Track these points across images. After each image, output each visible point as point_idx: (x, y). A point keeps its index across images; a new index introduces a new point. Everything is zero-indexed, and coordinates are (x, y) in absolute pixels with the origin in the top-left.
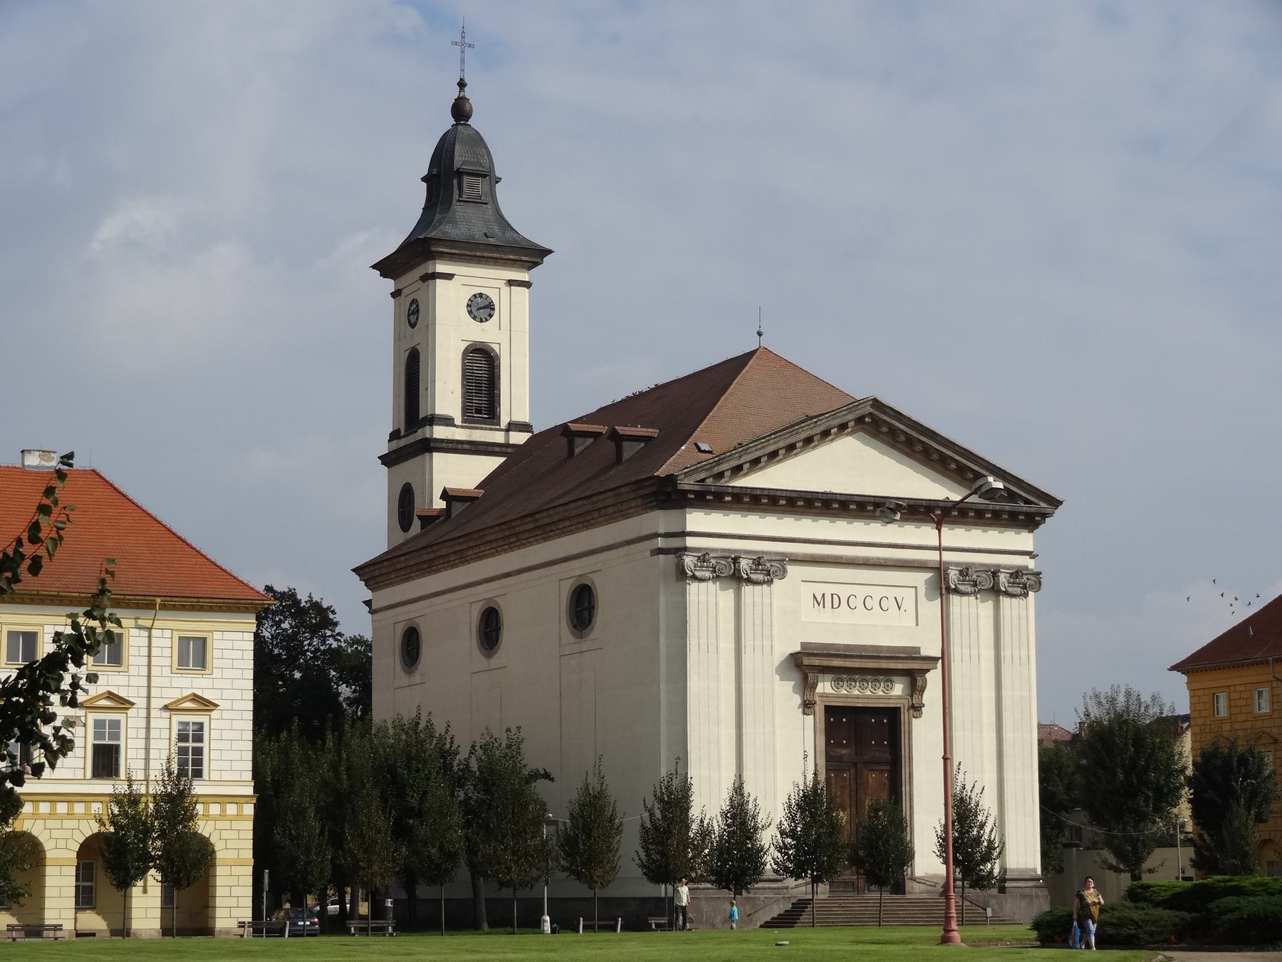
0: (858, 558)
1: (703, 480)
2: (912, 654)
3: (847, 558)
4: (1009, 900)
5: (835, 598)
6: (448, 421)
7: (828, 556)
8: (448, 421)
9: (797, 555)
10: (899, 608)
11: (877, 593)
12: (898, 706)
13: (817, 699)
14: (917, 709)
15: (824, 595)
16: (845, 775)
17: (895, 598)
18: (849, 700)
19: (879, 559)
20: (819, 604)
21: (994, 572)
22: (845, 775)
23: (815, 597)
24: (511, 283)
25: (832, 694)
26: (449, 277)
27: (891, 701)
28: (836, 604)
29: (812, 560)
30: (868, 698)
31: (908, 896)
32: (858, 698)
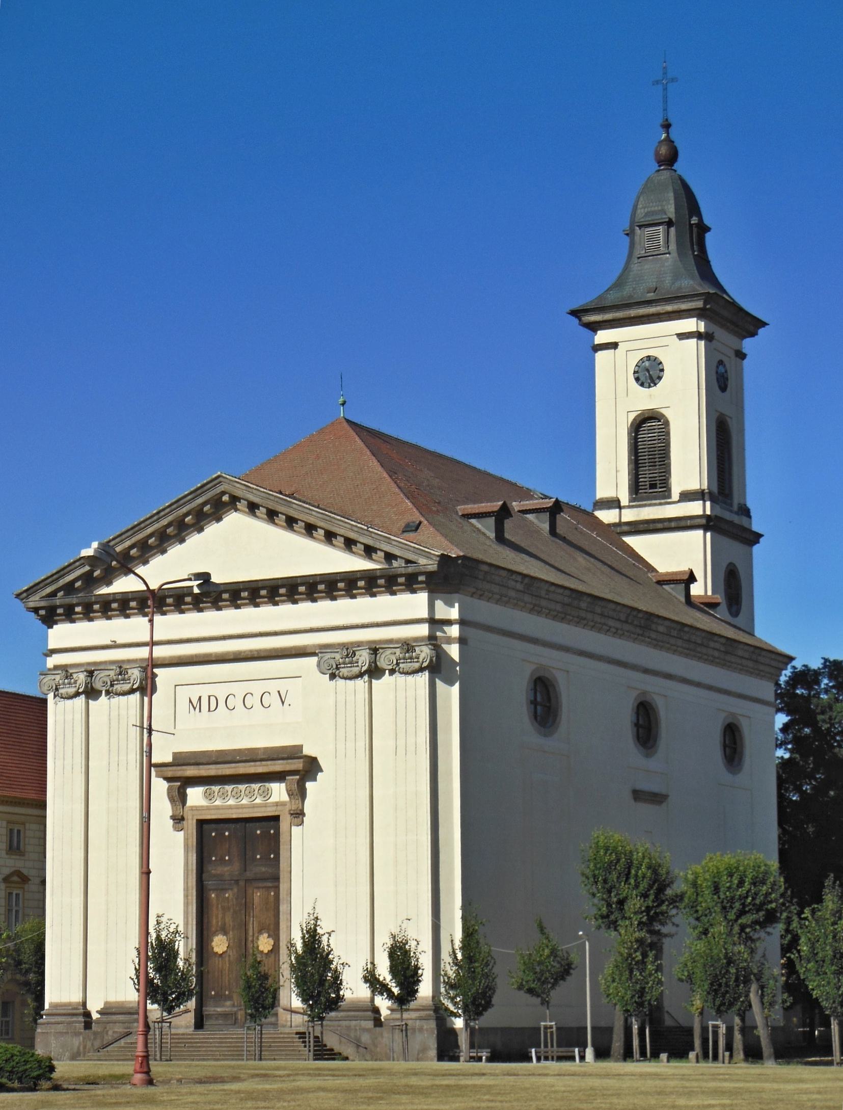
0: (228, 653)
1: (53, 594)
2: (294, 753)
3: (216, 655)
4: (385, 1035)
5: (213, 700)
6: (614, 503)
7: (196, 656)
8: (614, 503)
9: (164, 658)
10: (283, 703)
11: (257, 688)
12: (276, 814)
13: (188, 815)
14: (298, 815)
15: (200, 698)
16: (227, 895)
17: (279, 692)
18: (221, 811)
19: (251, 651)
20: (195, 709)
21: (375, 649)
22: (227, 895)
23: (190, 701)
24: (682, 336)
25: (202, 806)
26: (614, 346)
27: (269, 809)
28: (213, 707)
29: (179, 661)
30: (243, 807)
31: (281, 1030)
32: (231, 808)
